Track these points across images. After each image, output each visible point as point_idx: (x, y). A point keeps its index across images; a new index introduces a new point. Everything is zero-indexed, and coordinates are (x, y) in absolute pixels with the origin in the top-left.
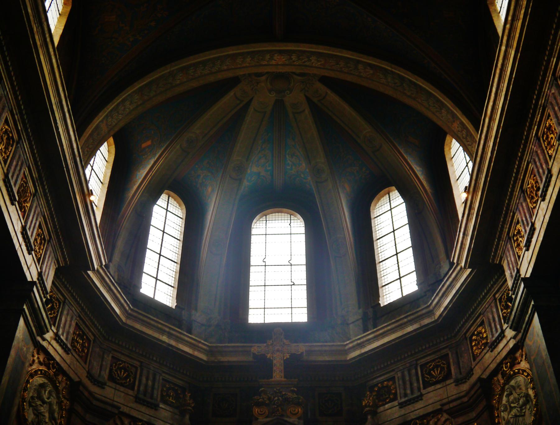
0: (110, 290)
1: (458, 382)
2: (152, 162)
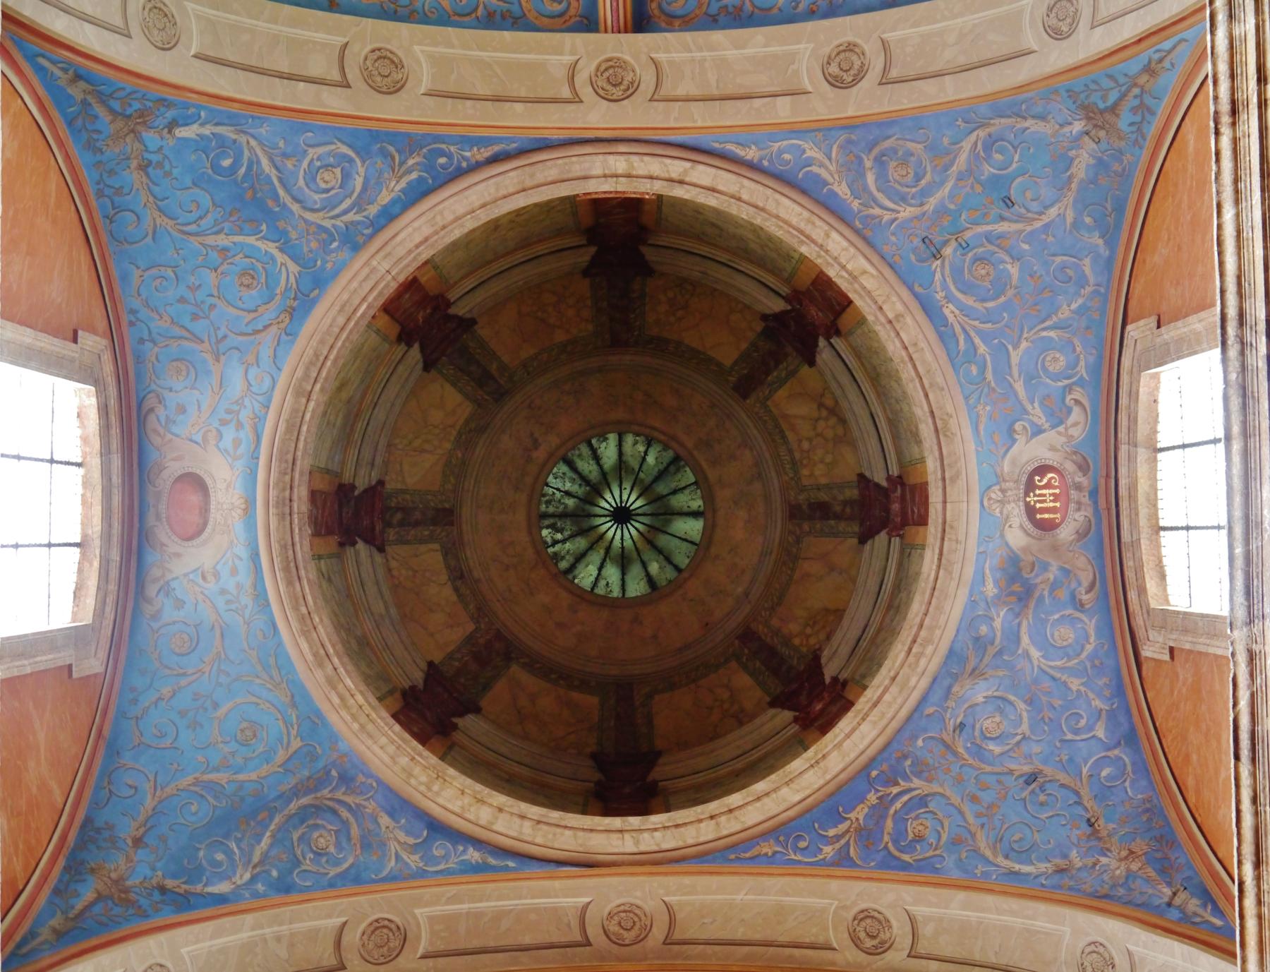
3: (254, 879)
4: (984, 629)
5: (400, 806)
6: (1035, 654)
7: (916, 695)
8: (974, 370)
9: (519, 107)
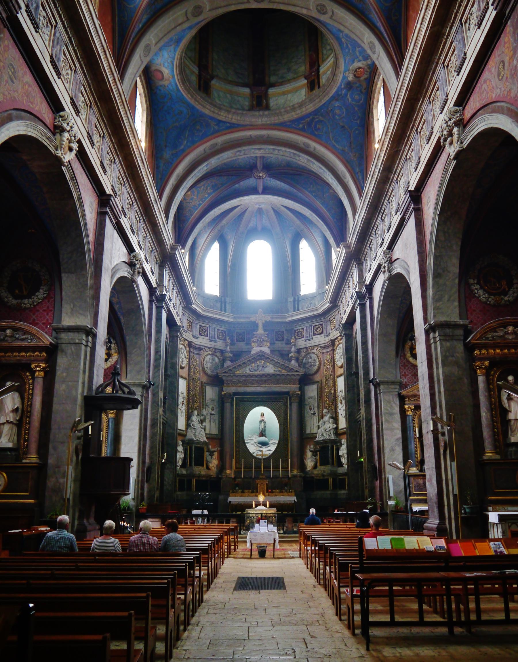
1: (325, 336)
2: (206, 236)
3: (187, 143)
4: (340, 93)
5: (212, 118)
6: (350, 99)
7: (322, 104)
8: (347, 50)
9: (233, 6)
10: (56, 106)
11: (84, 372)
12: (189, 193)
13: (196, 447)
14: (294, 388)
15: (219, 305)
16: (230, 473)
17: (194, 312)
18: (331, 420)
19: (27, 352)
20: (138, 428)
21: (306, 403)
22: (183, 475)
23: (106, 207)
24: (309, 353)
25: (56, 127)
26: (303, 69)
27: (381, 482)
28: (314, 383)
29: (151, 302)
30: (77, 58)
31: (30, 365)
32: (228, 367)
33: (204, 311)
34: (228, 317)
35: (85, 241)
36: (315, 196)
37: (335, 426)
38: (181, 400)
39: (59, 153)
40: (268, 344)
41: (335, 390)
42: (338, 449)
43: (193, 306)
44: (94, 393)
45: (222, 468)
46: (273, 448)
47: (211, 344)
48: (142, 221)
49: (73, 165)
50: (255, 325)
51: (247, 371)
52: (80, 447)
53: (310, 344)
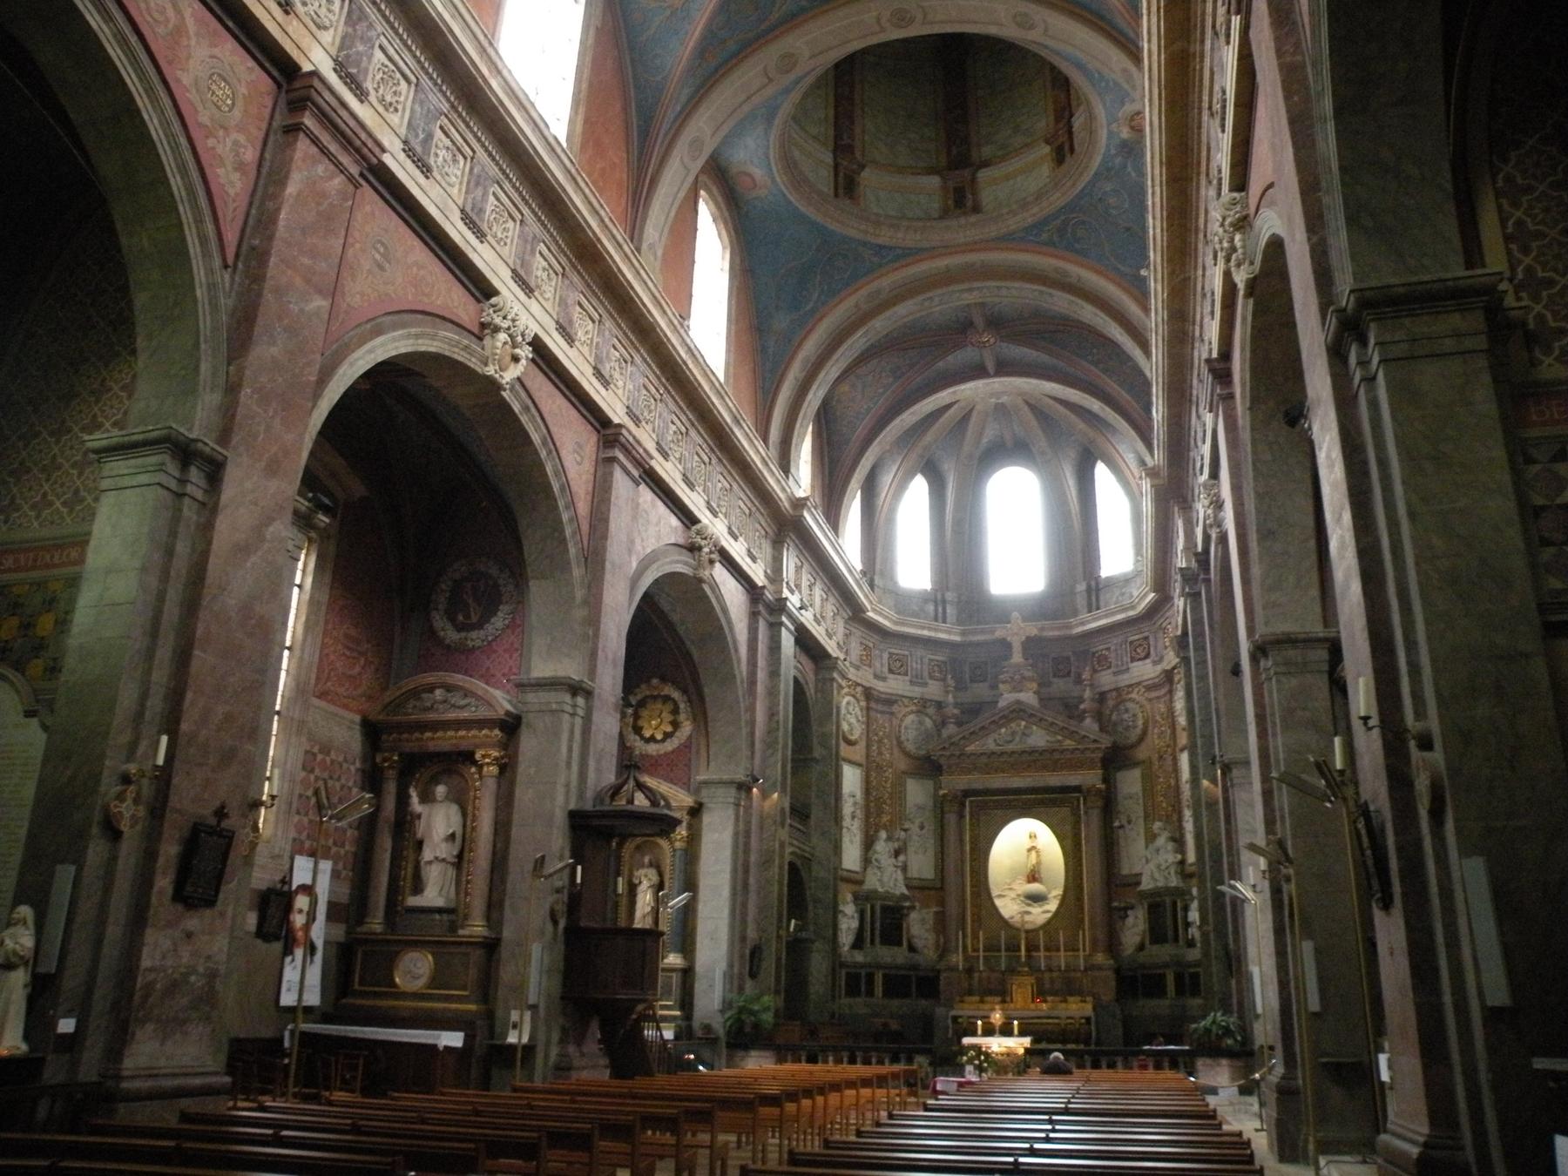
0: (880, 614)
1: (1155, 663)
5: (865, 244)
10: (482, 289)
11: (569, 764)
12: (845, 388)
13: (885, 909)
14: (1091, 778)
15: (931, 608)
16: (957, 959)
17: (873, 627)
18: (1170, 846)
19: (469, 729)
20: (728, 868)
21: (1120, 808)
22: (856, 965)
23: (613, 447)
24: (1124, 701)
25: (483, 326)
26: (1043, 123)
27: (1239, 982)
28: (1136, 764)
29: (754, 615)
30: (524, 199)
31: (472, 754)
32: (950, 737)
33: (896, 623)
34: (949, 633)
35: (565, 517)
36: (1105, 371)
37: (1179, 857)
38: (847, 809)
39: (490, 370)
40: (1035, 685)
41: (1177, 780)
42: (1186, 909)
43: (870, 614)
44: (589, 806)
45: (944, 951)
46: (1052, 906)
47: (917, 691)
48: (714, 461)
49: (528, 384)
50: (1005, 645)
51: (990, 744)
52: (561, 908)
53: (1125, 680)
